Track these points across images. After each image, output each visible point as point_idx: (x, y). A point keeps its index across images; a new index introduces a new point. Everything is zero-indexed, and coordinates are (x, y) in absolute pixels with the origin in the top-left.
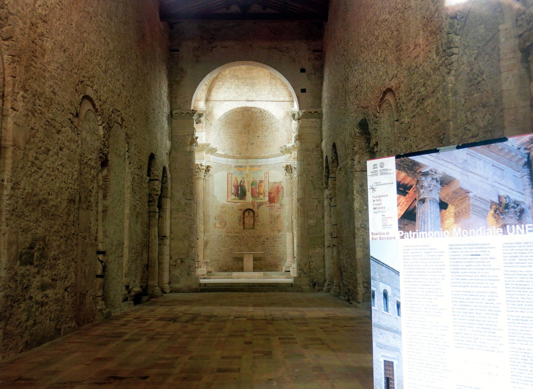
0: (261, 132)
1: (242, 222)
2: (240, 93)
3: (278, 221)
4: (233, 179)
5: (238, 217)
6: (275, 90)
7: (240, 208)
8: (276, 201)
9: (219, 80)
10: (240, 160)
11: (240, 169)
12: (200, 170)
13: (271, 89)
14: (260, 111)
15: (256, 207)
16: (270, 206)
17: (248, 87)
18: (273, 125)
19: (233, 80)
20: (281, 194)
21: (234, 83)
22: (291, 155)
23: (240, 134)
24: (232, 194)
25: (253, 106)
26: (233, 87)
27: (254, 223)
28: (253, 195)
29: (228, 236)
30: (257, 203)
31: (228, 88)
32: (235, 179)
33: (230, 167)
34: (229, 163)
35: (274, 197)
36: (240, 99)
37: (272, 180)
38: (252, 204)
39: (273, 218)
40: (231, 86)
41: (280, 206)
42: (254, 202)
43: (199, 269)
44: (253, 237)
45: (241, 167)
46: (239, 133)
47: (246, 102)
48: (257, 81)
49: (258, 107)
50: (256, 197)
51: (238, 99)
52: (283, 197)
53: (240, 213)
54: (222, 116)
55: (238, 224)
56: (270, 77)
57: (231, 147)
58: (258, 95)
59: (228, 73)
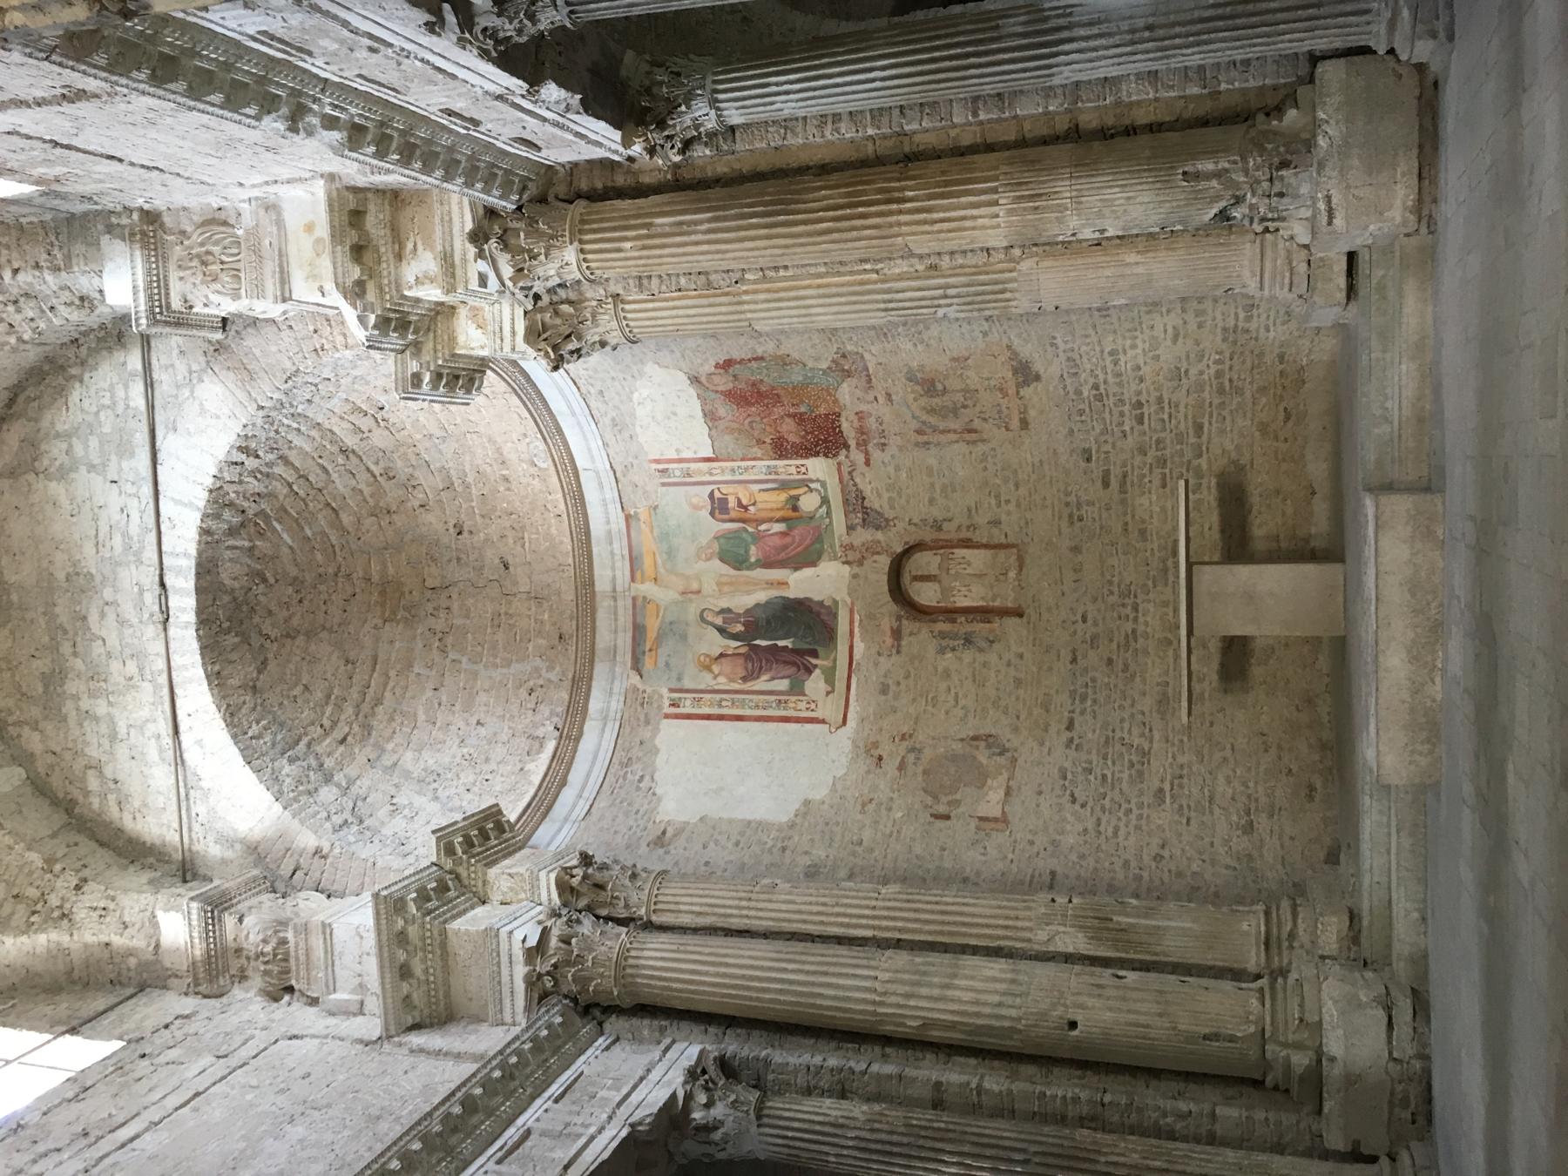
0: (430, 518)
1: (979, 627)
2: (132, 668)
3: (954, 384)
4: (706, 680)
5: (942, 651)
6: (94, 443)
7: (889, 641)
8: (822, 411)
9: (76, 794)
10: (603, 638)
11: (651, 634)
12: (568, 963)
13: (92, 468)
14: (232, 532)
15: (879, 535)
16: (862, 444)
17: (93, 618)
18: (351, 441)
19: (69, 707)
20: (769, 378)
21: (85, 704)
22: (463, 312)
23: (450, 640)
24: (797, 689)
25: (190, 584)
26: (101, 708)
27: (986, 546)
28: (807, 558)
29: (1070, 727)
30: (850, 528)
31: (113, 737)
32: (708, 668)
33: (636, 699)
34: (616, 705)
35: (800, 419)
36: (161, 664)
37: (696, 438)
38: (860, 563)
39: (942, 425)
40: (96, 719)
41: (848, 374)
42: (849, 547)
43: (1334, 1045)
44: (1076, 549)
45: (638, 630)
46: (443, 650)
47: (172, 631)
48: (59, 557)
49: (192, 550)
50: (819, 539)
51: (163, 680)
52: (784, 362)
53: (920, 637)
54: (274, 783)
55: (992, 658)
56: (31, 477)
57: (523, 693)
58: (128, 547)
59: (36, 736)
